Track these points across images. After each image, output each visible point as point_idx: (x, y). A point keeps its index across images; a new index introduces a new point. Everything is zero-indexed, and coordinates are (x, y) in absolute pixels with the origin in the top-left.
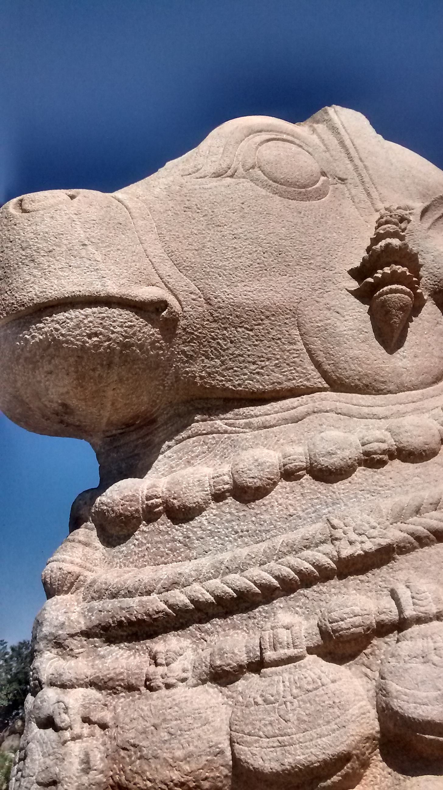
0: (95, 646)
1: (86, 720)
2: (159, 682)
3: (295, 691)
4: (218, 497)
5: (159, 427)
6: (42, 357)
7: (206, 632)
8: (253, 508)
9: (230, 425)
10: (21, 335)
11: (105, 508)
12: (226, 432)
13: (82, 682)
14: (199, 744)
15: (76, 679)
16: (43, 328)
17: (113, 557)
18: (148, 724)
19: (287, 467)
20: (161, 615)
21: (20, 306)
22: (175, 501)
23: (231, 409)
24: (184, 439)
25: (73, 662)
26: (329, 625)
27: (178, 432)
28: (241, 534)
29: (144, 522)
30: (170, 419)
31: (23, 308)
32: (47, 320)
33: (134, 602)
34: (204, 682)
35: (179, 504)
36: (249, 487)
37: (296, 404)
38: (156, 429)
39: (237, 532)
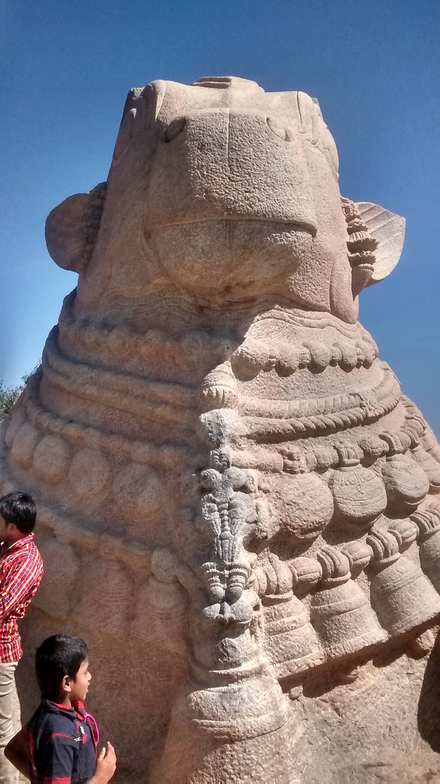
0: (251, 444)
1: (259, 488)
2: (298, 470)
3: (363, 480)
4: (301, 366)
5: (256, 305)
6: (278, 255)
7: (306, 444)
8: (317, 378)
9: (291, 318)
10: (274, 235)
11: (250, 357)
12: (289, 322)
13: (253, 466)
14: (326, 503)
15: (250, 463)
16: (289, 237)
17: (244, 389)
18: (300, 492)
19: (334, 358)
20: (290, 431)
21: (284, 217)
22: (286, 363)
23: (293, 308)
24: (266, 318)
25: (240, 453)
26: (371, 450)
27: (264, 311)
28: (312, 391)
29: (262, 371)
30: (263, 302)
31: (285, 219)
32: (293, 233)
34: (311, 471)
35: (288, 366)
36: (320, 365)
37: (321, 317)
38: (255, 306)
39: (309, 390)
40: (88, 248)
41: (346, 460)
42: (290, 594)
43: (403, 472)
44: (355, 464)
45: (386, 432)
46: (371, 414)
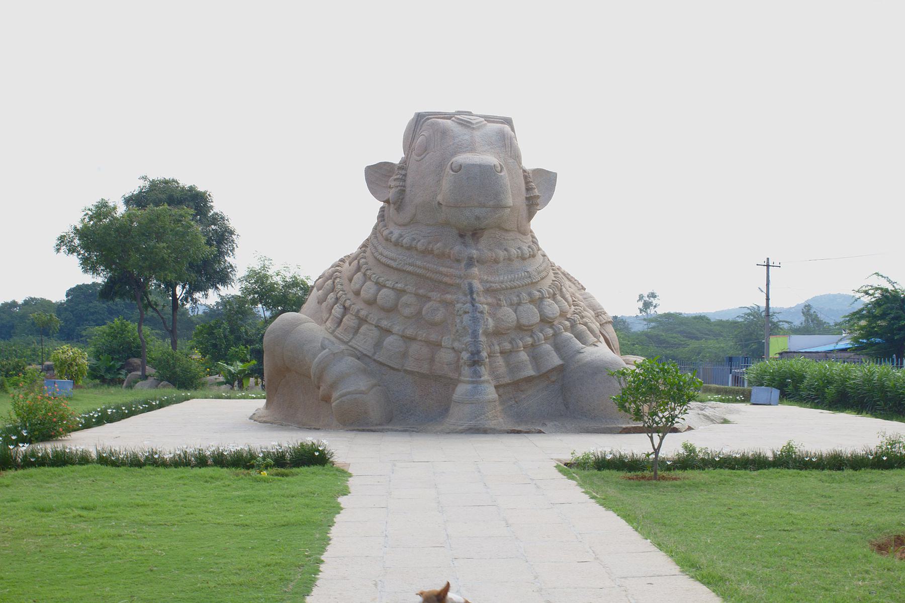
33: (493, 285)
40: (401, 197)
41: (523, 302)
42: (499, 355)
43: (547, 307)
44: (526, 303)
45: (541, 289)
46: (534, 281)
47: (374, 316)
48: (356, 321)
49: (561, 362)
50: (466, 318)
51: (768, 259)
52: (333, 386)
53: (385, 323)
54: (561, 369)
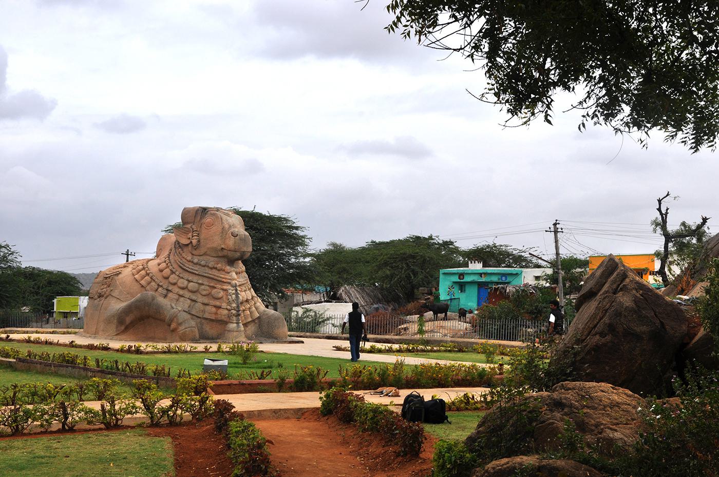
47: (187, 294)
48: (177, 296)
49: (259, 315)
50: (234, 296)
51: (128, 250)
52: (180, 324)
53: (194, 298)
54: (259, 318)
